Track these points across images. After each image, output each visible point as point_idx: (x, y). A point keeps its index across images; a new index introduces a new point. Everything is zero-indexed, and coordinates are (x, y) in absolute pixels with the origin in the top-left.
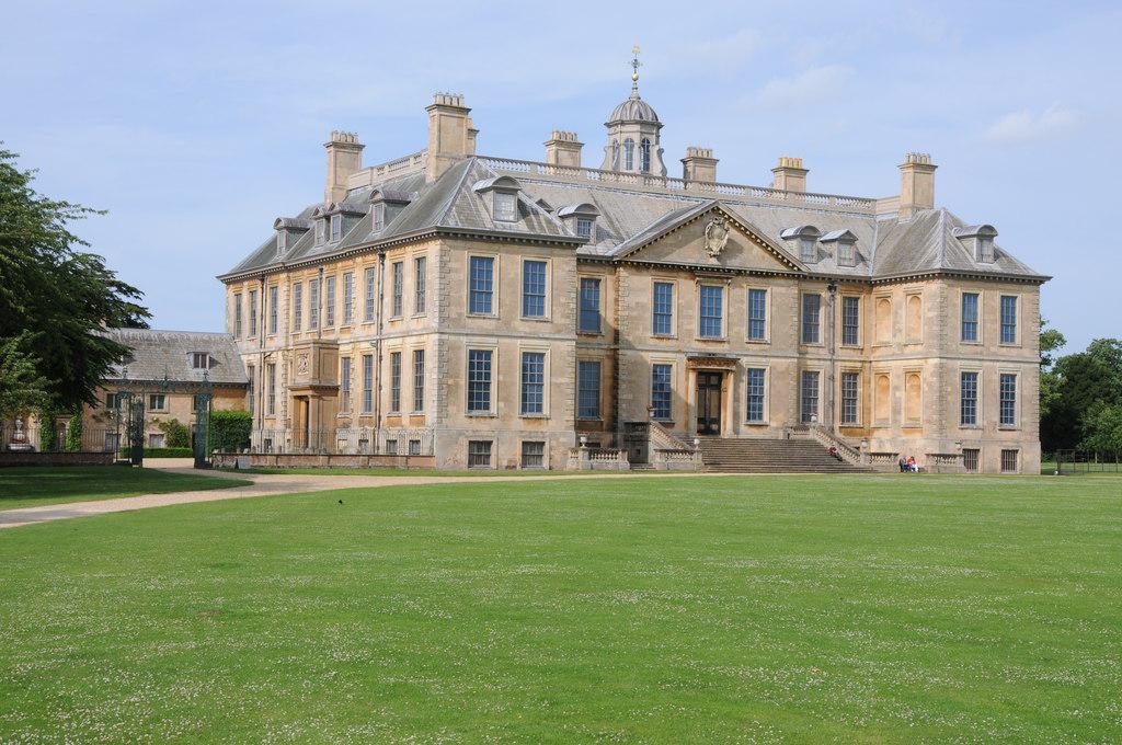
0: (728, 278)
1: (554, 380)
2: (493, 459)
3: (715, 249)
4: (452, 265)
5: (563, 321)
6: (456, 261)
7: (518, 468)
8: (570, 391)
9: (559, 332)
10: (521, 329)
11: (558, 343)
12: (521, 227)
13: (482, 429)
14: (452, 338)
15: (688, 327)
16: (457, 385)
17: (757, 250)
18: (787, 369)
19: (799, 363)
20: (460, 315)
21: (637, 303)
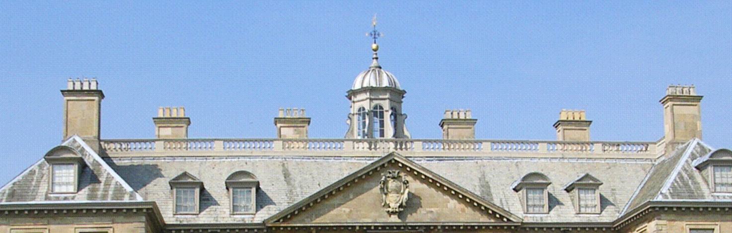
3: (392, 205)
12: (82, 198)
17: (453, 203)
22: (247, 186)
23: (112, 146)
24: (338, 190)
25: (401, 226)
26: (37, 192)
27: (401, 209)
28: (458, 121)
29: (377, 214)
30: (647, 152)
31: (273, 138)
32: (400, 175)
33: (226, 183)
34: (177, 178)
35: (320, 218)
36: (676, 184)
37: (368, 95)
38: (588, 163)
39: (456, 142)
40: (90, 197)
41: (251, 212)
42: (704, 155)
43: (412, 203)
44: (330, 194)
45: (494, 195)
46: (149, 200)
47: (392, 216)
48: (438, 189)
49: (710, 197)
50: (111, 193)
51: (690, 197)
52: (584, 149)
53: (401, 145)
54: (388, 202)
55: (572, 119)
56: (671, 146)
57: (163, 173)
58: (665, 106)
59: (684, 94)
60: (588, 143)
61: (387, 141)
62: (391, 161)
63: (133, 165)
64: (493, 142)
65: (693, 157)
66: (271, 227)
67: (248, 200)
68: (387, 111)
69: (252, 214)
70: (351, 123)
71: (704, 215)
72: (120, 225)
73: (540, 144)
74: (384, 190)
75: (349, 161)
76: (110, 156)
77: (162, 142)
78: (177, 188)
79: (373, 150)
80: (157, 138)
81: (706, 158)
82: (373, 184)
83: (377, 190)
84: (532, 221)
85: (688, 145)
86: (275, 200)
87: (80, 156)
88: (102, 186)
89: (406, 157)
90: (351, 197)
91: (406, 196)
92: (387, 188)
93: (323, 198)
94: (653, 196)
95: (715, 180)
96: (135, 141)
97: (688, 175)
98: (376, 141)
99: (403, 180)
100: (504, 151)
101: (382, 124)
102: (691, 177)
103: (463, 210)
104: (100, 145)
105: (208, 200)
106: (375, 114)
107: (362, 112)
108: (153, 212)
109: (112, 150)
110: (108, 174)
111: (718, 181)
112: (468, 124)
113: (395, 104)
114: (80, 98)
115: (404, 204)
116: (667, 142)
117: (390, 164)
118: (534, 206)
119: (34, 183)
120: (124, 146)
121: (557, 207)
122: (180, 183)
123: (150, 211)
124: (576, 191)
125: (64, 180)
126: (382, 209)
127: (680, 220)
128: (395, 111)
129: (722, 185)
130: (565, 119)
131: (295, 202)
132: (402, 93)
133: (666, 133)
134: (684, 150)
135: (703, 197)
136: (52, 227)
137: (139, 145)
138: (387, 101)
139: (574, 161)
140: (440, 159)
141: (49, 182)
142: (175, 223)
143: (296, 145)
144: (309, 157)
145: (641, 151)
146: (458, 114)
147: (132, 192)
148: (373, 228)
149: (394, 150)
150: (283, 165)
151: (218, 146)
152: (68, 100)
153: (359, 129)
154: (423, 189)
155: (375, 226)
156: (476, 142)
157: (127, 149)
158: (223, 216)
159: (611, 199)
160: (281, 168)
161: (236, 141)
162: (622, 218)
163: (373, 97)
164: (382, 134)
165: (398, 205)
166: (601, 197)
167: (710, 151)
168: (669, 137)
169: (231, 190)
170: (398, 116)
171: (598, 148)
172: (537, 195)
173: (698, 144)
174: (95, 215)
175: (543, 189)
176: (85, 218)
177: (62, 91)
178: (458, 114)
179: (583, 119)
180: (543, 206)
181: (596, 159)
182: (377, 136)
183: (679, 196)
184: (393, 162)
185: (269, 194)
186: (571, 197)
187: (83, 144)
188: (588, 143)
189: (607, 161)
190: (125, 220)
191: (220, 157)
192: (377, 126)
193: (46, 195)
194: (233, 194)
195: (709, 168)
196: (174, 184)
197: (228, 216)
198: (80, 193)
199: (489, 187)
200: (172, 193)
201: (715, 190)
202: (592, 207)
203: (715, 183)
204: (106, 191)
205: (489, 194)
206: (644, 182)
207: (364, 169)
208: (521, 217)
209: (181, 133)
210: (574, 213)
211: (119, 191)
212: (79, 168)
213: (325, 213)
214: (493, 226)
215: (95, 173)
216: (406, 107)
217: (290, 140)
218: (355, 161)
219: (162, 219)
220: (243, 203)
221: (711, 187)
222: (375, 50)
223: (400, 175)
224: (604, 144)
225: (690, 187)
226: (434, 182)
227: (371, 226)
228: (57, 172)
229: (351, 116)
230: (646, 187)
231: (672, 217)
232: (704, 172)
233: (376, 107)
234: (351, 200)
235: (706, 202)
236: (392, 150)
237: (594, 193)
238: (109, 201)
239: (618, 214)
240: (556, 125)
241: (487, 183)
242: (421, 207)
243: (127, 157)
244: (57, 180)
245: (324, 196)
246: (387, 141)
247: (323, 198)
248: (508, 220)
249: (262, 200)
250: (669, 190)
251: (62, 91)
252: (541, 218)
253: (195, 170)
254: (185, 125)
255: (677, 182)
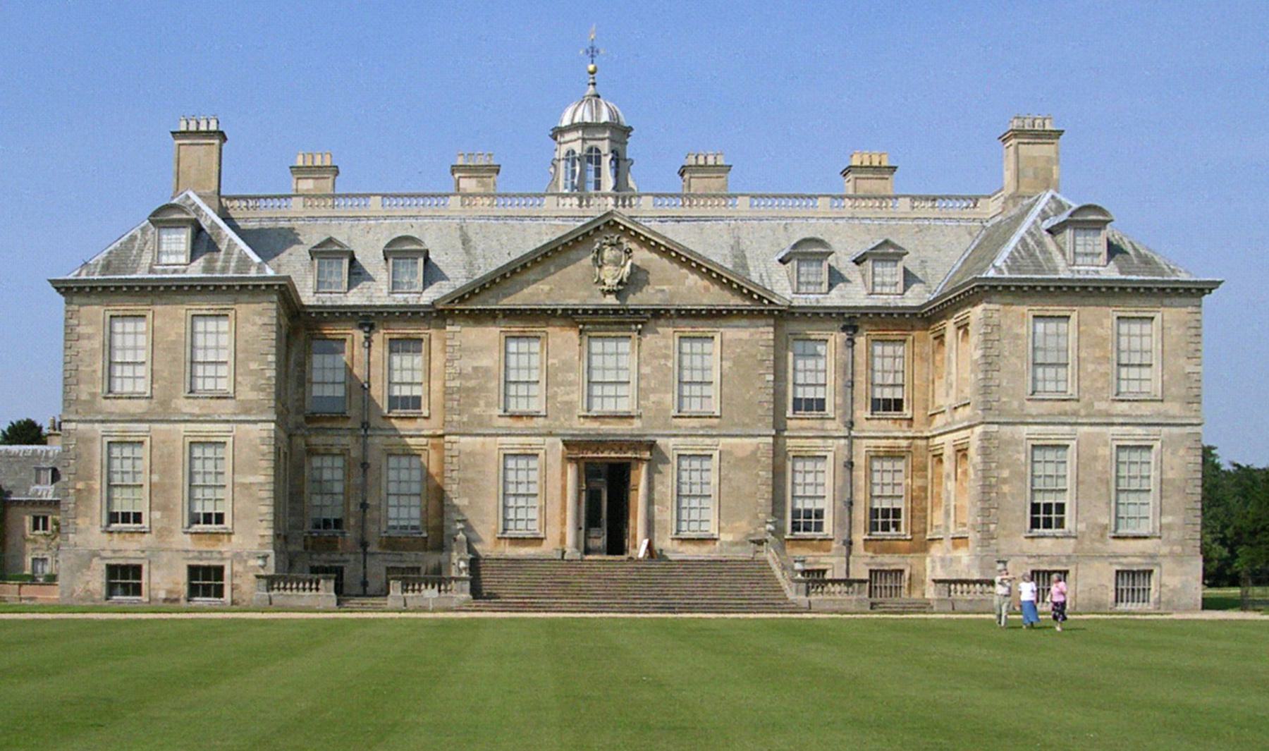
0: (636, 323)
1: (240, 479)
2: (144, 588)
3: (608, 281)
4: (82, 330)
5: (253, 396)
6: (90, 323)
7: (183, 603)
8: (267, 494)
9: (247, 411)
10: (185, 410)
11: (247, 426)
12: (196, 271)
13: (128, 549)
14: (81, 426)
15: (566, 398)
16: (90, 490)
17: (693, 279)
18: (754, 453)
19: (775, 444)
20: (94, 395)
21: (475, 369)
22: (413, 255)
23: (236, 203)
24: (535, 261)
25: (619, 310)
26: (138, 264)
27: (620, 287)
28: (705, 168)
29: (586, 294)
30: (977, 210)
31: (450, 192)
32: (621, 240)
33: (384, 251)
34: (319, 246)
35: (510, 299)
36: (1016, 254)
37: (580, 134)
38: (889, 226)
39: (701, 196)
40: (205, 270)
41: (417, 290)
42: (1060, 213)
43: (637, 278)
44: (524, 267)
45: (751, 269)
46: (283, 274)
47: (608, 296)
48: (672, 259)
49: (1068, 272)
50: (233, 264)
51: (1036, 272)
52: (884, 204)
53: (624, 201)
54: (602, 278)
55: (868, 164)
56: (1011, 201)
57: (300, 238)
58: (1008, 144)
59: (1036, 128)
60: (889, 197)
61: (605, 196)
62: (608, 222)
63: (262, 229)
64: (753, 197)
65: (1044, 216)
66: (442, 310)
67: (414, 274)
68: (605, 155)
69: (417, 293)
70: (556, 170)
71: (1057, 296)
72: (244, 306)
73: (820, 199)
74: (598, 262)
75: (553, 222)
76: (233, 216)
77: (302, 198)
78: (319, 258)
79: (585, 208)
80: (294, 193)
81: (1064, 216)
82: (582, 253)
83: (588, 261)
84: (804, 304)
85: (1037, 200)
86: (448, 273)
87: (193, 216)
88: (221, 256)
89: (631, 217)
90: (552, 270)
91: (627, 269)
92: (602, 259)
93: (514, 272)
94: (982, 270)
95: (1075, 249)
96: (266, 198)
97: (1036, 242)
98: (589, 197)
99: (625, 248)
100: (766, 208)
101: (598, 173)
102: (1040, 244)
103: (707, 289)
104: (220, 202)
105: (359, 274)
106: (589, 160)
107: (571, 156)
108: (287, 289)
109: (237, 210)
110: (230, 240)
111: (1079, 249)
112: (719, 172)
113: (617, 146)
114: (196, 141)
115: (625, 280)
116: (1007, 195)
117: (608, 226)
118: (808, 283)
119: (134, 252)
120: (251, 203)
121: (841, 285)
122: (325, 252)
123: (283, 289)
124: (869, 263)
125: (174, 247)
126: (594, 287)
127: (1019, 304)
128: (617, 155)
129: (1086, 254)
130: (859, 164)
131: (477, 277)
132: (627, 131)
133: (1006, 182)
134: (1032, 206)
135: (1056, 271)
136: (158, 308)
137: (270, 203)
138: (607, 142)
139: (868, 222)
140: (678, 220)
141: (153, 250)
142: (315, 303)
143: (480, 201)
144: (497, 218)
145: (967, 207)
146: (706, 158)
147: (260, 263)
148: (580, 312)
149: (614, 208)
150: (462, 228)
151: (375, 202)
152: (180, 145)
153: (566, 180)
154: (651, 260)
155: (584, 310)
156: (729, 196)
157: (255, 208)
158: (379, 294)
159: (919, 275)
160: (459, 233)
161: (406, 196)
162: (936, 300)
163: (586, 136)
164: (598, 185)
165: (617, 281)
166: (906, 271)
167: (1070, 207)
168: (1010, 188)
169: (391, 261)
170: (621, 162)
171: (904, 204)
172: (813, 269)
173: (1053, 197)
174: (213, 292)
175: (822, 261)
176: (199, 297)
177: (172, 133)
178: (706, 158)
179: (884, 164)
180: (821, 284)
181: (900, 219)
182: (591, 189)
183: (1019, 270)
184: (612, 223)
185: (440, 265)
186: (861, 271)
187: (199, 202)
188: (889, 197)
189: (915, 222)
190: (251, 300)
191: (377, 218)
192: (591, 175)
193: (150, 267)
194: (394, 265)
195: (1068, 231)
196: (313, 253)
197: (386, 294)
198: (193, 264)
199: (745, 257)
200: (313, 265)
201: (1075, 262)
202: (891, 285)
203: (1075, 253)
204: (227, 261)
205: (745, 267)
206: (970, 251)
207: (571, 233)
208: (788, 298)
209: (326, 185)
210: (865, 293)
211: (244, 262)
212: (193, 233)
213: (517, 292)
214: (748, 310)
215: (214, 238)
216: (632, 149)
217: (471, 195)
218: (561, 223)
219: (298, 298)
220: (406, 279)
221: (1068, 257)
222: (592, 73)
223: (621, 240)
224: (913, 198)
225: (1037, 258)
226: (668, 250)
227: (577, 310)
228: (165, 237)
229: (555, 162)
230: (972, 257)
231: (1009, 299)
232: (1059, 238)
233: (590, 150)
234: (553, 274)
235: (1060, 279)
236: (610, 208)
237: (896, 266)
238: (230, 274)
239: (928, 295)
240: (845, 173)
241: (743, 251)
242: (649, 284)
243: (253, 219)
244: (164, 247)
245: (515, 269)
246: (605, 196)
247: (514, 272)
248: (770, 302)
249: (432, 274)
250: (1005, 261)
251: (172, 133)
252: (818, 301)
253: (343, 234)
254: (332, 177)
255: (1019, 252)
